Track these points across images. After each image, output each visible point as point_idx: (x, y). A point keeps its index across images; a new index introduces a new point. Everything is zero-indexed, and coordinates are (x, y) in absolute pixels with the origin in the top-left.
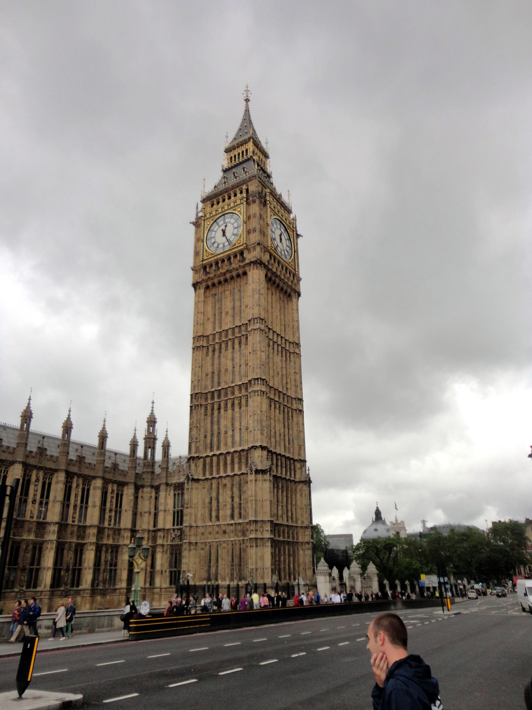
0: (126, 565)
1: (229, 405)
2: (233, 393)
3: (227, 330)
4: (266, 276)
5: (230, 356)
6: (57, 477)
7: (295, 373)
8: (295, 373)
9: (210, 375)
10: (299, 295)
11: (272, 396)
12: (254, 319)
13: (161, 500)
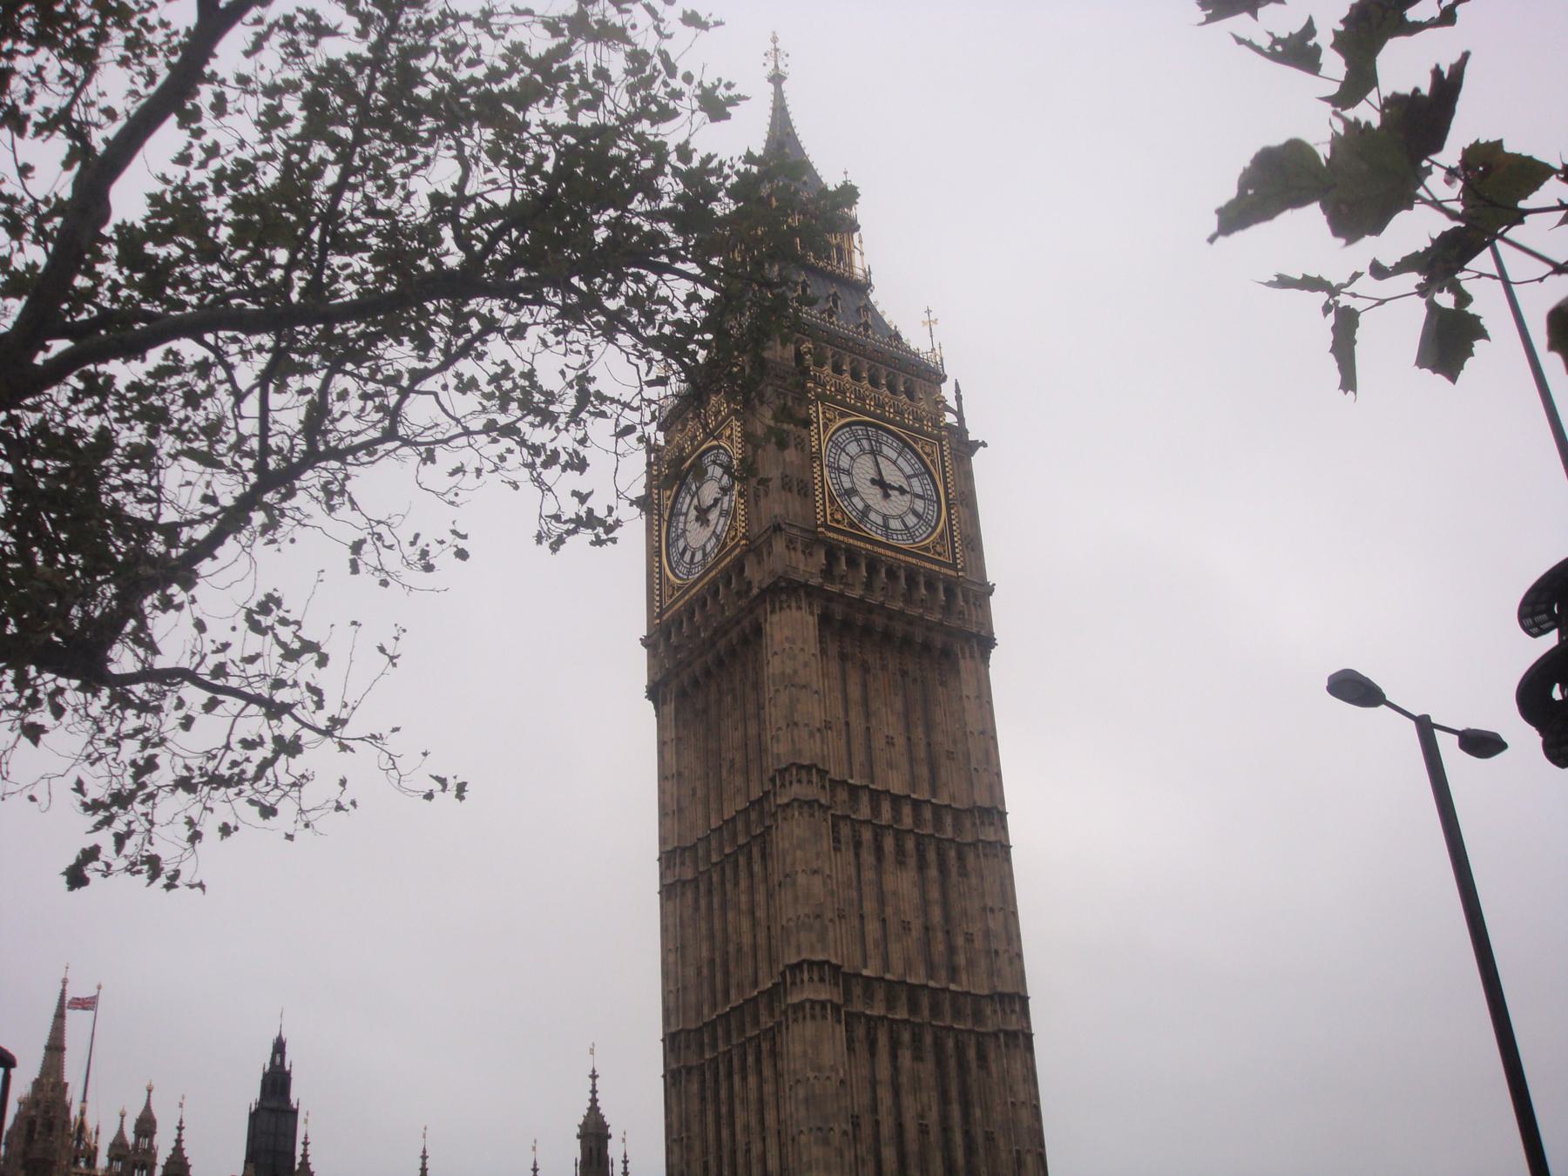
1: (750, 1060)
2: (756, 1021)
3: (734, 818)
4: (825, 620)
7: (984, 909)
8: (984, 909)
9: (705, 971)
11: (878, 1010)
12: (782, 772)
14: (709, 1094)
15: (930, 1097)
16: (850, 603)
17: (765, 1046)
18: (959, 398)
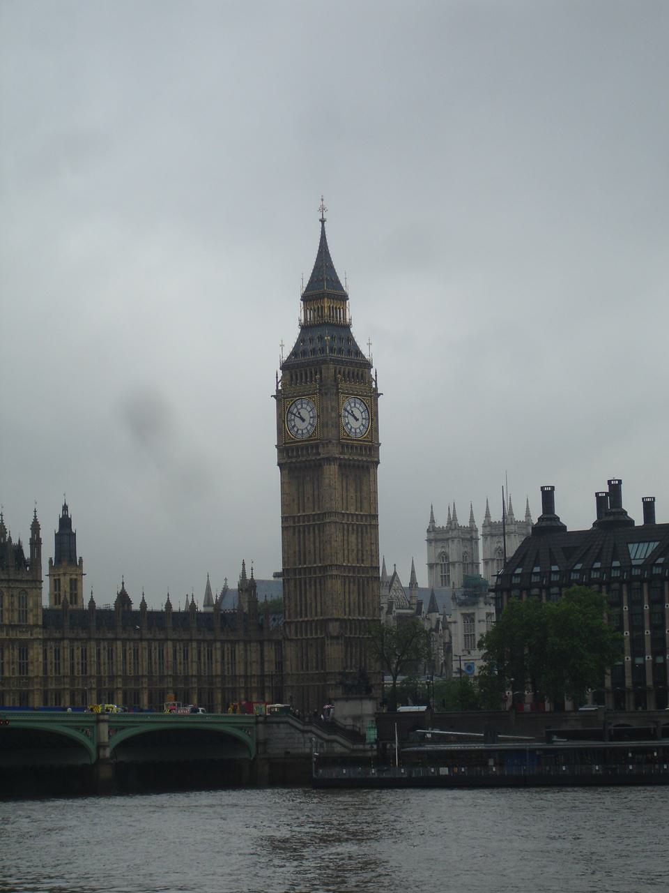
1: (313, 582)
2: (315, 573)
5: (312, 540)
6: (192, 645)
9: (297, 554)
10: (378, 462)
13: (266, 653)
14: (298, 587)
15: (356, 595)
17: (318, 581)
18: (376, 376)
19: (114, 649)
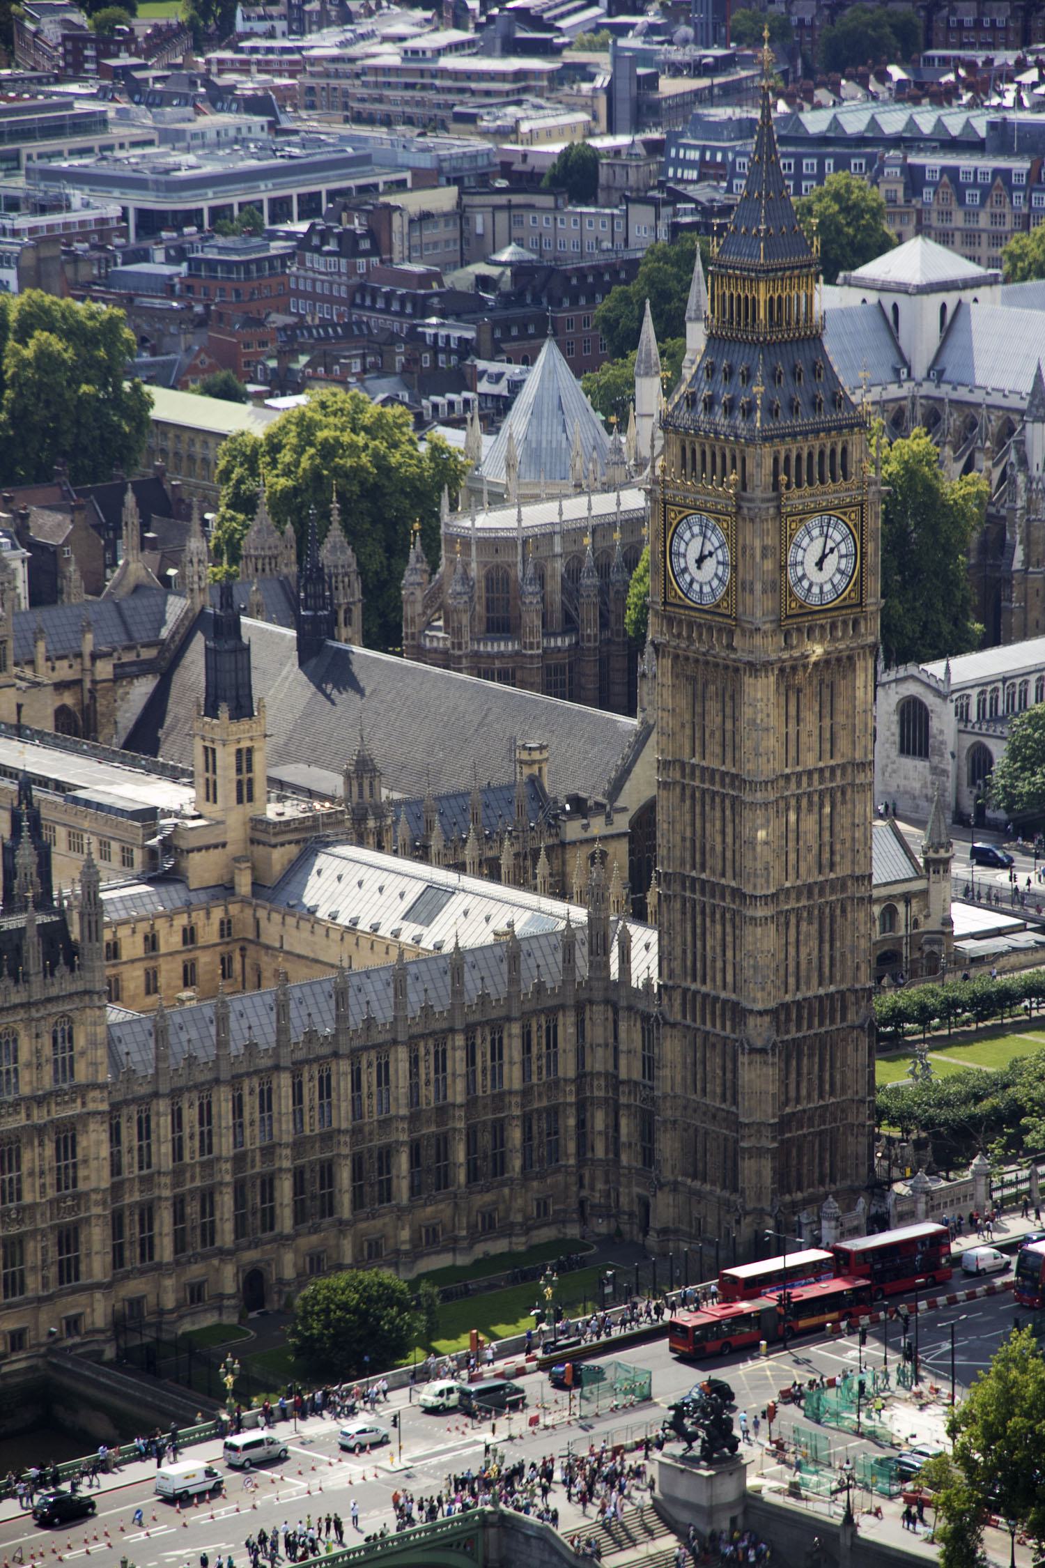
0: (572, 1132)
1: (718, 916)
5: (718, 824)
8: (853, 824)
9: (688, 844)
13: (623, 1035)
14: (689, 916)
15: (814, 943)
16: (796, 659)
19: (274, 1086)
